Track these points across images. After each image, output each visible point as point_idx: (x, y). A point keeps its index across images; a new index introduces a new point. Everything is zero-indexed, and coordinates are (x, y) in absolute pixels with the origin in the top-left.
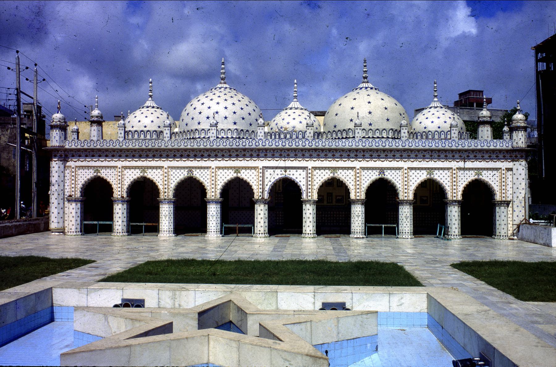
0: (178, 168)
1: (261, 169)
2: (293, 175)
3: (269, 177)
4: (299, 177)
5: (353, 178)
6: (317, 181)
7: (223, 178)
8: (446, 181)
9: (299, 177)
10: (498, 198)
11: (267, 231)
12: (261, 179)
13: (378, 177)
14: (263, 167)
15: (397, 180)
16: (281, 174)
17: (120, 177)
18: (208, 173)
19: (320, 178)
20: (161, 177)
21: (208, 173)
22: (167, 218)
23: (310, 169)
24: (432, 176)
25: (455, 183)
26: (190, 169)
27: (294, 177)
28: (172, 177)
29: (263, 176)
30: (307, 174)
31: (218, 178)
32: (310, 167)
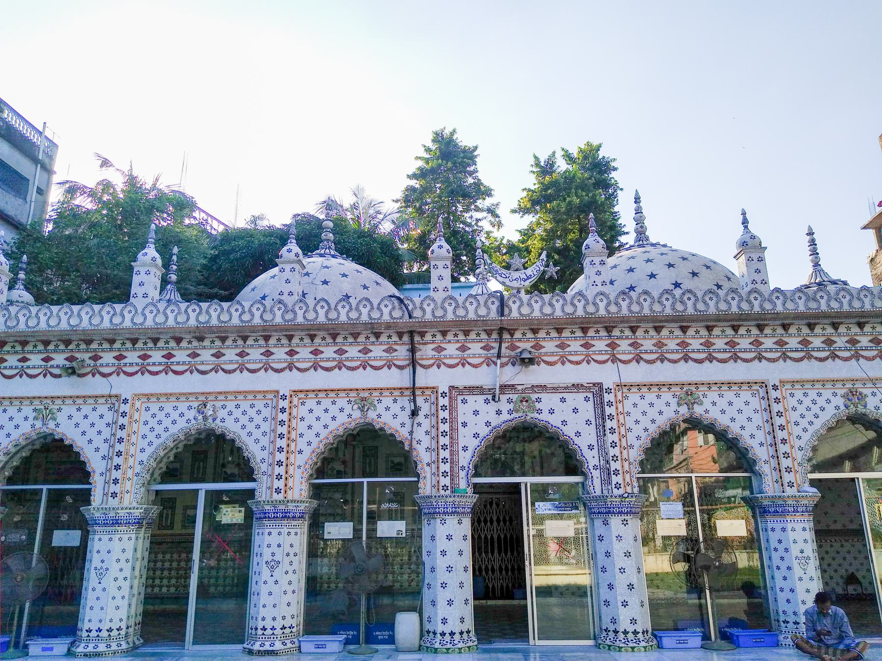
0: (168, 396)
1: (444, 394)
2: (552, 412)
3: (470, 419)
4: (570, 417)
5: (758, 419)
7: (318, 427)
9: (570, 417)
11: (469, 624)
13: (843, 412)
14: (452, 388)
16: (510, 412)
18: (266, 412)
19: (645, 422)
21: (266, 412)
23: (609, 391)
26: (203, 400)
27: (554, 421)
29: (453, 420)
30: (600, 405)
31: (302, 427)
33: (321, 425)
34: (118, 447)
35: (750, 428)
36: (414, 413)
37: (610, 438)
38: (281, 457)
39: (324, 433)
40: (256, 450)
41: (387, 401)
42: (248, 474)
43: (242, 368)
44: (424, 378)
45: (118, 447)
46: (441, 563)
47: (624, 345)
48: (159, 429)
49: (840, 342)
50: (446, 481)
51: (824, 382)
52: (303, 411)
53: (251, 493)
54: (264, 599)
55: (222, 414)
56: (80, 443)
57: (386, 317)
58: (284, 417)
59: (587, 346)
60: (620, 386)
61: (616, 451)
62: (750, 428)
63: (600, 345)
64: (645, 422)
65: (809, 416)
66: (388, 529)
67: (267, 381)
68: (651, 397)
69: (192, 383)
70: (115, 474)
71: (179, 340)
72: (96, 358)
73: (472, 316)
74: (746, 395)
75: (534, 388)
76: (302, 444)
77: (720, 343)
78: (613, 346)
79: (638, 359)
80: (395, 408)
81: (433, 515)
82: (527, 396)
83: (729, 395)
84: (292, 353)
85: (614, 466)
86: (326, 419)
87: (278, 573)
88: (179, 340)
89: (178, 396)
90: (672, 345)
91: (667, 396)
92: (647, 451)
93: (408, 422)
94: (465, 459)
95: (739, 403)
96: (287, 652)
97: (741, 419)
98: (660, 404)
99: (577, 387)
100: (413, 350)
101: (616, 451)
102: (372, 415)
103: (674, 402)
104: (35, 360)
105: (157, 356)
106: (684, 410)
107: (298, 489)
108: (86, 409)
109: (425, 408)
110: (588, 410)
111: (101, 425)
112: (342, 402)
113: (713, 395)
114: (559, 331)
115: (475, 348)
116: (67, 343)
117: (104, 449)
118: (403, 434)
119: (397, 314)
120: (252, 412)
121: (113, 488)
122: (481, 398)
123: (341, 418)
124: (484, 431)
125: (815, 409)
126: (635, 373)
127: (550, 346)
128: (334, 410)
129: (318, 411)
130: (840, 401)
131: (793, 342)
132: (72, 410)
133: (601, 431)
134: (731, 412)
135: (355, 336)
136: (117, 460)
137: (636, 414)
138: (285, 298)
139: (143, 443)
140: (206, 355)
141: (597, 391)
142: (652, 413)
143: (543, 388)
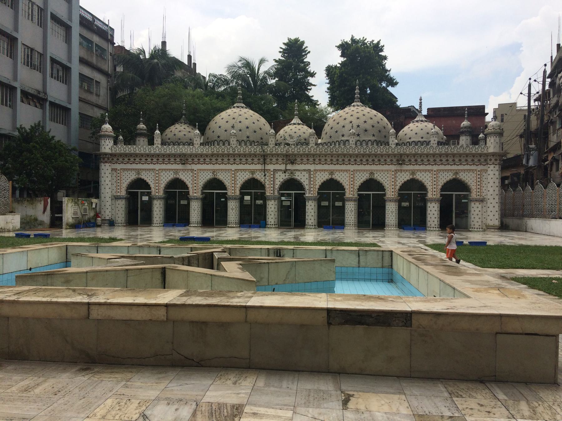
3: (278, 177)
4: (303, 177)
5: (348, 179)
6: (318, 181)
7: (241, 178)
8: (427, 181)
10: (474, 195)
12: (272, 179)
15: (386, 181)
17: (158, 178)
18: (229, 174)
19: (320, 179)
20: (191, 178)
22: (196, 212)
24: (415, 176)
25: (435, 183)
26: (214, 171)
27: (299, 178)
28: (200, 178)
29: (274, 177)
30: (310, 175)
31: (238, 178)
32: (312, 169)
33: (243, 177)
34: (195, 182)
35: (345, 181)
36: (265, 176)
37: (312, 183)
38: (233, 185)
39: (243, 180)
40: (227, 182)
41: (258, 172)
42: (226, 189)
43: (223, 163)
44: (269, 167)
45: (195, 182)
46: (270, 210)
47: (317, 160)
48: (204, 178)
49: (370, 160)
50: (272, 192)
51: (364, 170)
52: (238, 174)
53: (226, 193)
54: (231, 216)
55: (218, 174)
56: (185, 180)
57: (258, 152)
58: (233, 176)
59: (308, 160)
60: (315, 170)
61: (312, 186)
62: (345, 181)
63: (311, 159)
64: (320, 179)
65: (360, 178)
66: (259, 202)
67: (228, 167)
68: (322, 173)
69: (210, 167)
70: (195, 188)
71: (207, 156)
72: (187, 160)
73: (279, 152)
74: (345, 173)
75: (294, 170)
76: (238, 182)
77: (340, 160)
78: (314, 160)
79: (320, 163)
80: (260, 174)
81: (269, 199)
82: (292, 172)
83: (341, 173)
84: (235, 160)
85: (312, 189)
86: (243, 176)
87: (234, 211)
88: (207, 156)
89: (208, 170)
90: (329, 160)
91: (326, 173)
92: (320, 186)
93: (264, 178)
94: (277, 187)
95: (343, 175)
96: (237, 227)
97: (343, 179)
98: (324, 175)
99: (304, 170)
100: (265, 160)
101: (312, 186)
102: (254, 176)
103: (328, 174)
104: (172, 160)
105: (202, 160)
106: (330, 176)
107: (238, 193)
108: (186, 172)
109: (267, 174)
110: (307, 175)
111: (190, 176)
112: (247, 172)
113: (337, 173)
114: (301, 156)
115: (280, 159)
116: (180, 156)
117: (191, 182)
118: (262, 180)
119: (261, 150)
120: (225, 174)
121: (195, 191)
122: (281, 172)
123: (247, 176)
124: (282, 180)
125: (362, 177)
126: (319, 167)
127: (299, 159)
128: (245, 174)
129: (242, 174)
130: (368, 175)
131: (358, 160)
132: (182, 172)
133: (310, 181)
134: (341, 177)
135: (250, 156)
136: (195, 185)
137: (318, 177)
138: (232, 145)
139: (200, 181)
140: (214, 160)
141: (309, 171)
142: (322, 177)
143: (297, 170)
